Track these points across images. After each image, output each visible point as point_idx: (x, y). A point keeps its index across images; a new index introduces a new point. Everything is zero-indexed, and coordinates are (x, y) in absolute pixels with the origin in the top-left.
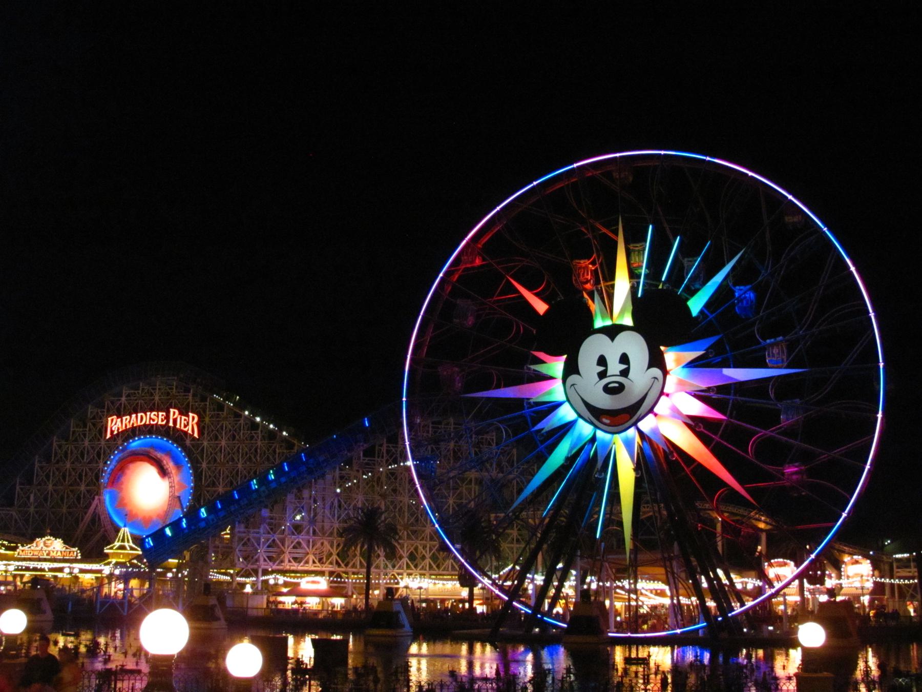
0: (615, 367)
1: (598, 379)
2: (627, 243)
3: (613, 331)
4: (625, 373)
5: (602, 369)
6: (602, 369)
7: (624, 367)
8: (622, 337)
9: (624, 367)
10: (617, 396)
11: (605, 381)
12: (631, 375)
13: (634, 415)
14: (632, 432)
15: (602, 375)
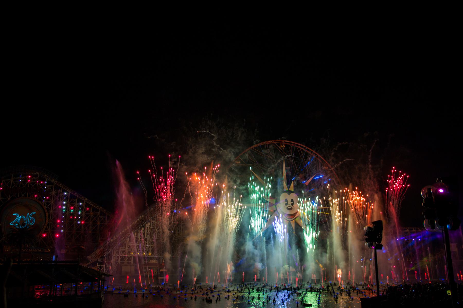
0: (290, 203)
1: (285, 205)
2: (285, 167)
3: (289, 192)
4: (292, 204)
5: (286, 202)
6: (286, 202)
7: (292, 203)
8: (292, 194)
9: (293, 203)
10: (291, 210)
11: (287, 206)
12: (294, 205)
13: (294, 217)
14: (294, 221)
15: (286, 204)
